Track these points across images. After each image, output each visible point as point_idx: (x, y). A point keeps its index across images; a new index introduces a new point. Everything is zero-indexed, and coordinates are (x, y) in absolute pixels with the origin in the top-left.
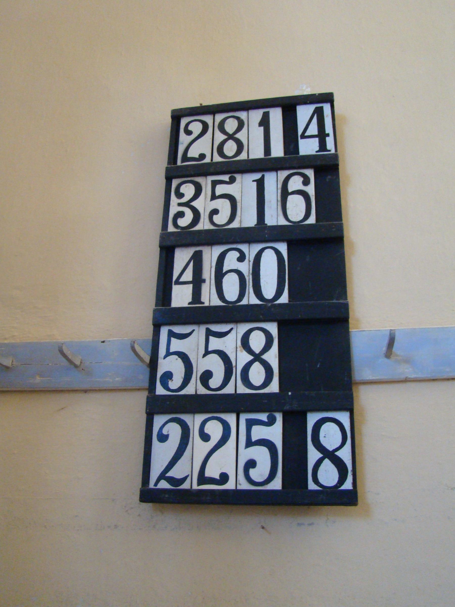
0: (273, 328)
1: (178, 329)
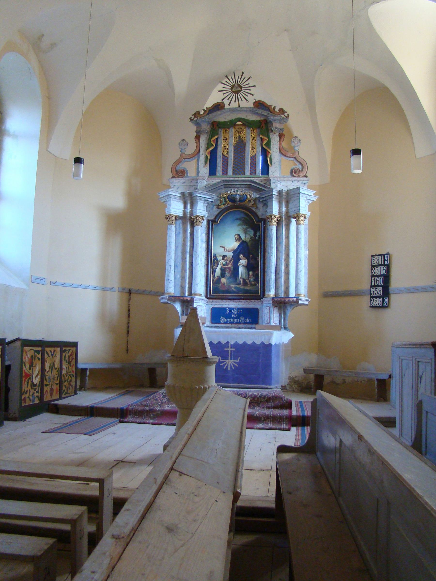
0: (381, 288)
1: (373, 288)
